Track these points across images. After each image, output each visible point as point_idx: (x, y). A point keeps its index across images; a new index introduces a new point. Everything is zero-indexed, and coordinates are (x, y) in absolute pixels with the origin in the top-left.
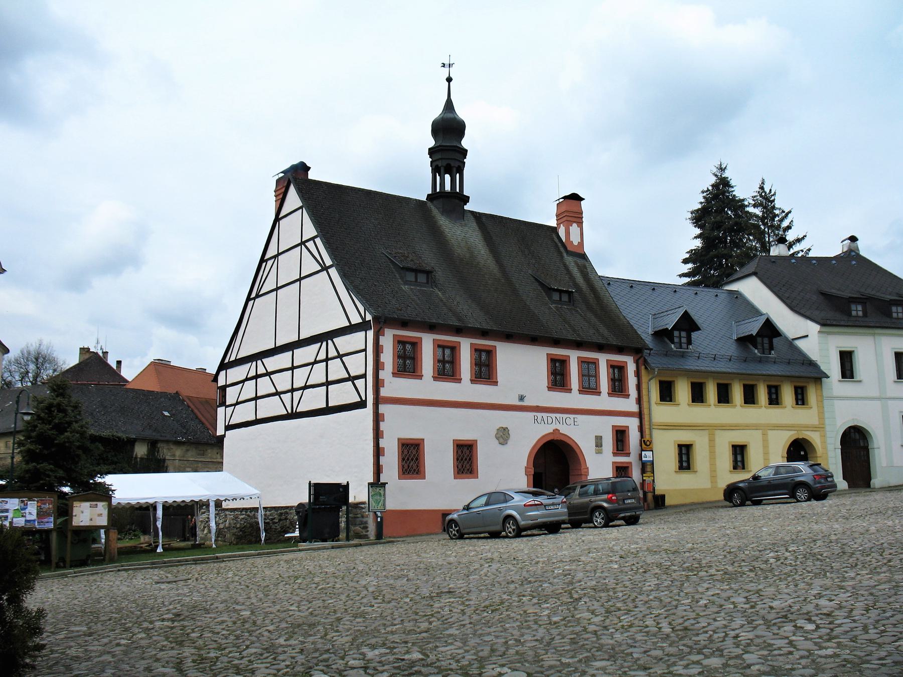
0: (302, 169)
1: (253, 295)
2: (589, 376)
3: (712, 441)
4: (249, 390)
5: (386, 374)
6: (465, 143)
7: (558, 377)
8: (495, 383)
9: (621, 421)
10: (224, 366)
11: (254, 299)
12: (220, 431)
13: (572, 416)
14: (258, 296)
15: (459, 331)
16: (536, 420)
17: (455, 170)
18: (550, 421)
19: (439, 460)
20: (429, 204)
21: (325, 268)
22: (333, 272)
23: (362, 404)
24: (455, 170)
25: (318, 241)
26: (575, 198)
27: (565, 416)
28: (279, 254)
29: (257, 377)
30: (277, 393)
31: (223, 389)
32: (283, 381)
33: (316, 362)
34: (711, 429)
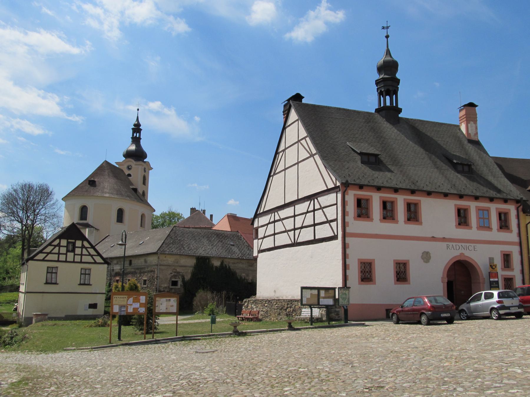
0: (298, 98)
1: (272, 174)
2: (484, 218)
4: (270, 230)
5: (350, 218)
6: (398, 76)
7: (462, 218)
8: (421, 224)
9: (507, 248)
10: (257, 215)
11: (273, 176)
12: (255, 254)
13: (473, 245)
14: (275, 174)
15: (396, 190)
16: (448, 247)
17: (392, 92)
18: (458, 248)
19: (384, 273)
20: (377, 116)
21: (312, 155)
22: (317, 157)
23: (334, 238)
24: (392, 92)
25: (308, 139)
26: (472, 105)
27: (468, 245)
28: (286, 149)
29: (275, 222)
30: (286, 231)
31: (257, 230)
32: (289, 224)
33: (308, 212)
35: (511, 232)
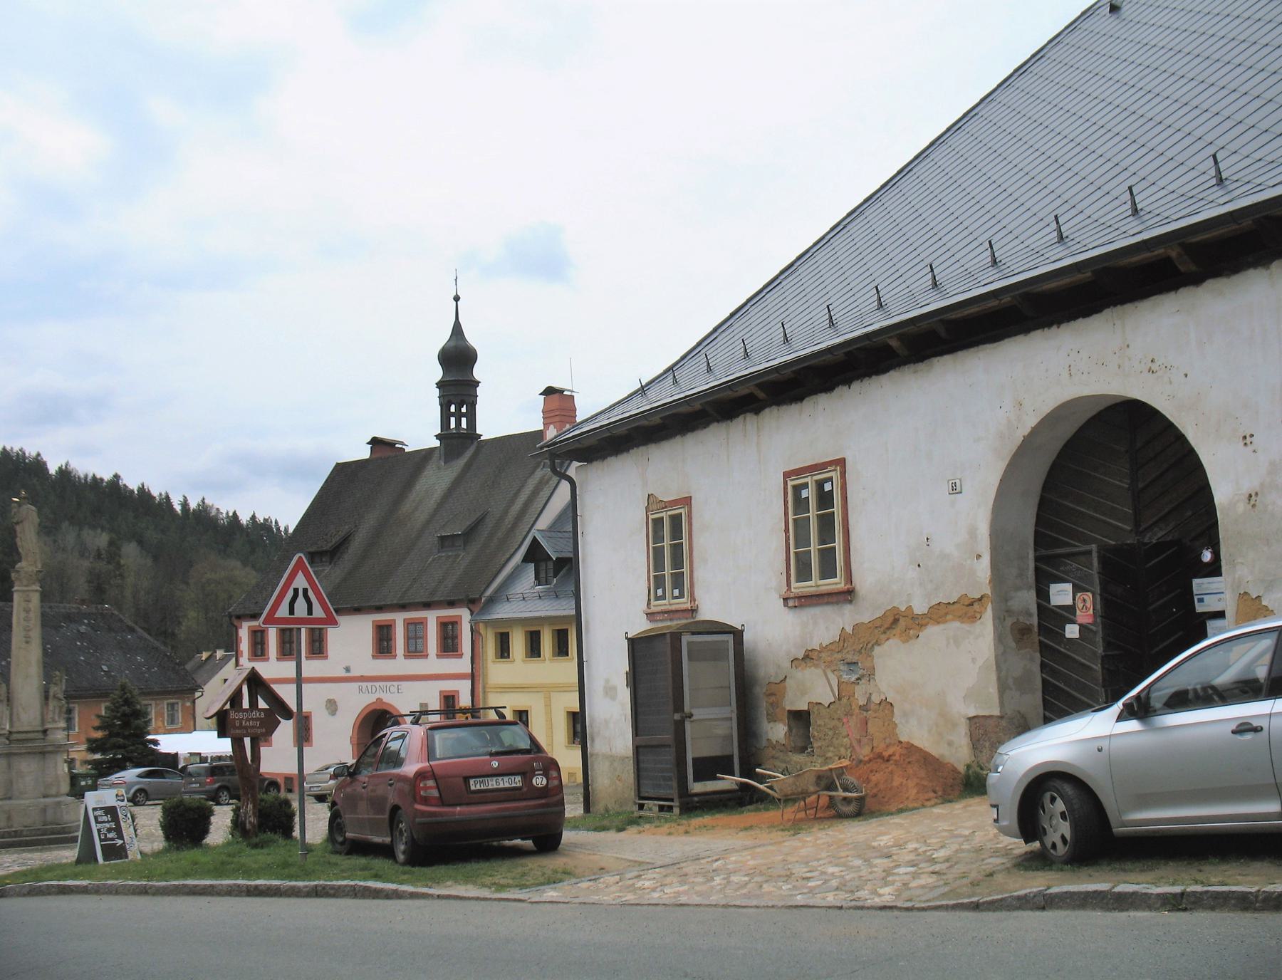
3: (548, 705)
7: (383, 644)
9: (449, 686)
13: (395, 684)
16: (360, 690)
27: (389, 684)
34: (547, 690)
35: (461, 656)
